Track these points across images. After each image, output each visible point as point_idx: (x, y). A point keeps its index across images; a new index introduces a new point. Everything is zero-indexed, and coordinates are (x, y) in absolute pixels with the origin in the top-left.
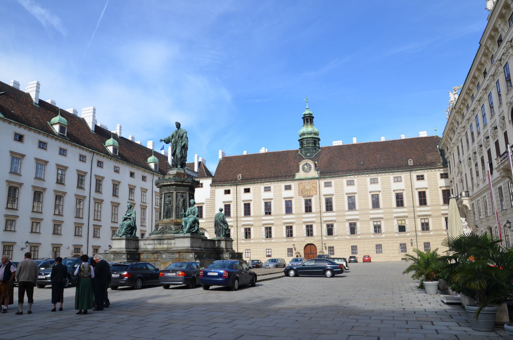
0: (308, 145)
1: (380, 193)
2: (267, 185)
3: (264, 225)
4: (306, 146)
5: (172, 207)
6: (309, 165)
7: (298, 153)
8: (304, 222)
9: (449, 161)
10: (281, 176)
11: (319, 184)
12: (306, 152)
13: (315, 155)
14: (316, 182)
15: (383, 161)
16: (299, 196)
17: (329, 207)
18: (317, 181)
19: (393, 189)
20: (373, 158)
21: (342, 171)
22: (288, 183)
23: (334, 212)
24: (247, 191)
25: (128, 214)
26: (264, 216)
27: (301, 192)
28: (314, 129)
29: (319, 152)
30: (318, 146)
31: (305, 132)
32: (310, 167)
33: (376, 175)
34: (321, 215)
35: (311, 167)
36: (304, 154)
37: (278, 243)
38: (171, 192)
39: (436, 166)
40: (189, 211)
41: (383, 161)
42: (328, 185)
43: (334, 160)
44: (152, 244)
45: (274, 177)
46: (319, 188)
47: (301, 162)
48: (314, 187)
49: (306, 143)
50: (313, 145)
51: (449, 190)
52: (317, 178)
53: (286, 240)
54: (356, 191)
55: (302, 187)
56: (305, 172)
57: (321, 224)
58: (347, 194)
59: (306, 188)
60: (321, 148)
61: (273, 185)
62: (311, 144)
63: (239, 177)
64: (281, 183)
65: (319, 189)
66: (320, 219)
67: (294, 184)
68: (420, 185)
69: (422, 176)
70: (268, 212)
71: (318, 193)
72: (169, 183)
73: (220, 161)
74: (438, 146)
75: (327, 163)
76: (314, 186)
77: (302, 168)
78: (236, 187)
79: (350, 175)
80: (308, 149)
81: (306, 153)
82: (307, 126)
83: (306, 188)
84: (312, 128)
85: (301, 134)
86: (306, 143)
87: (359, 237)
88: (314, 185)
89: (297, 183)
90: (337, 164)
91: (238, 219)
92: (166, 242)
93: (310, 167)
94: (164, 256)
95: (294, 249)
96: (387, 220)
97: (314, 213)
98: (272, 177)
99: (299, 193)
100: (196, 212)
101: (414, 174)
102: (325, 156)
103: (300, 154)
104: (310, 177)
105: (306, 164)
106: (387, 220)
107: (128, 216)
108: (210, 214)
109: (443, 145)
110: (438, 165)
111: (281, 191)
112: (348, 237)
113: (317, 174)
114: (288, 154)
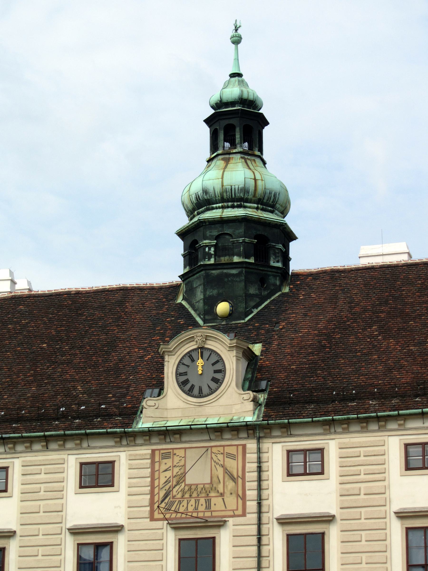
0: (224, 260)
4: (212, 261)
6: (214, 359)
7: (175, 297)
10: (64, 416)
11: (259, 458)
12: (215, 292)
13: (255, 311)
14: (244, 446)
16: (152, 519)
28: (258, 177)
29: (284, 294)
30: (280, 265)
31: (211, 190)
32: (218, 367)
35: (222, 371)
36: (201, 305)
43: (352, 339)
45: (31, 420)
46: (260, 480)
47: (173, 344)
49: (216, 246)
50: (252, 260)
55: (168, 474)
56: (190, 392)
59: (190, 479)
60: (296, 275)
62: (239, 255)
64: (63, 448)
65: (260, 488)
75: (312, 353)
76: (236, 477)
77: (178, 374)
80: (220, 278)
82: (227, 161)
83: (190, 479)
84: (249, 174)
85: (194, 200)
86: (216, 246)
88: (231, 464)
89: (146, 451)
90: (365, 354)
93: (216, 372)
102: (305, 315)
103: (184, 303)
104: (212, 421)
113: (250, 406)
114: (121, 303)
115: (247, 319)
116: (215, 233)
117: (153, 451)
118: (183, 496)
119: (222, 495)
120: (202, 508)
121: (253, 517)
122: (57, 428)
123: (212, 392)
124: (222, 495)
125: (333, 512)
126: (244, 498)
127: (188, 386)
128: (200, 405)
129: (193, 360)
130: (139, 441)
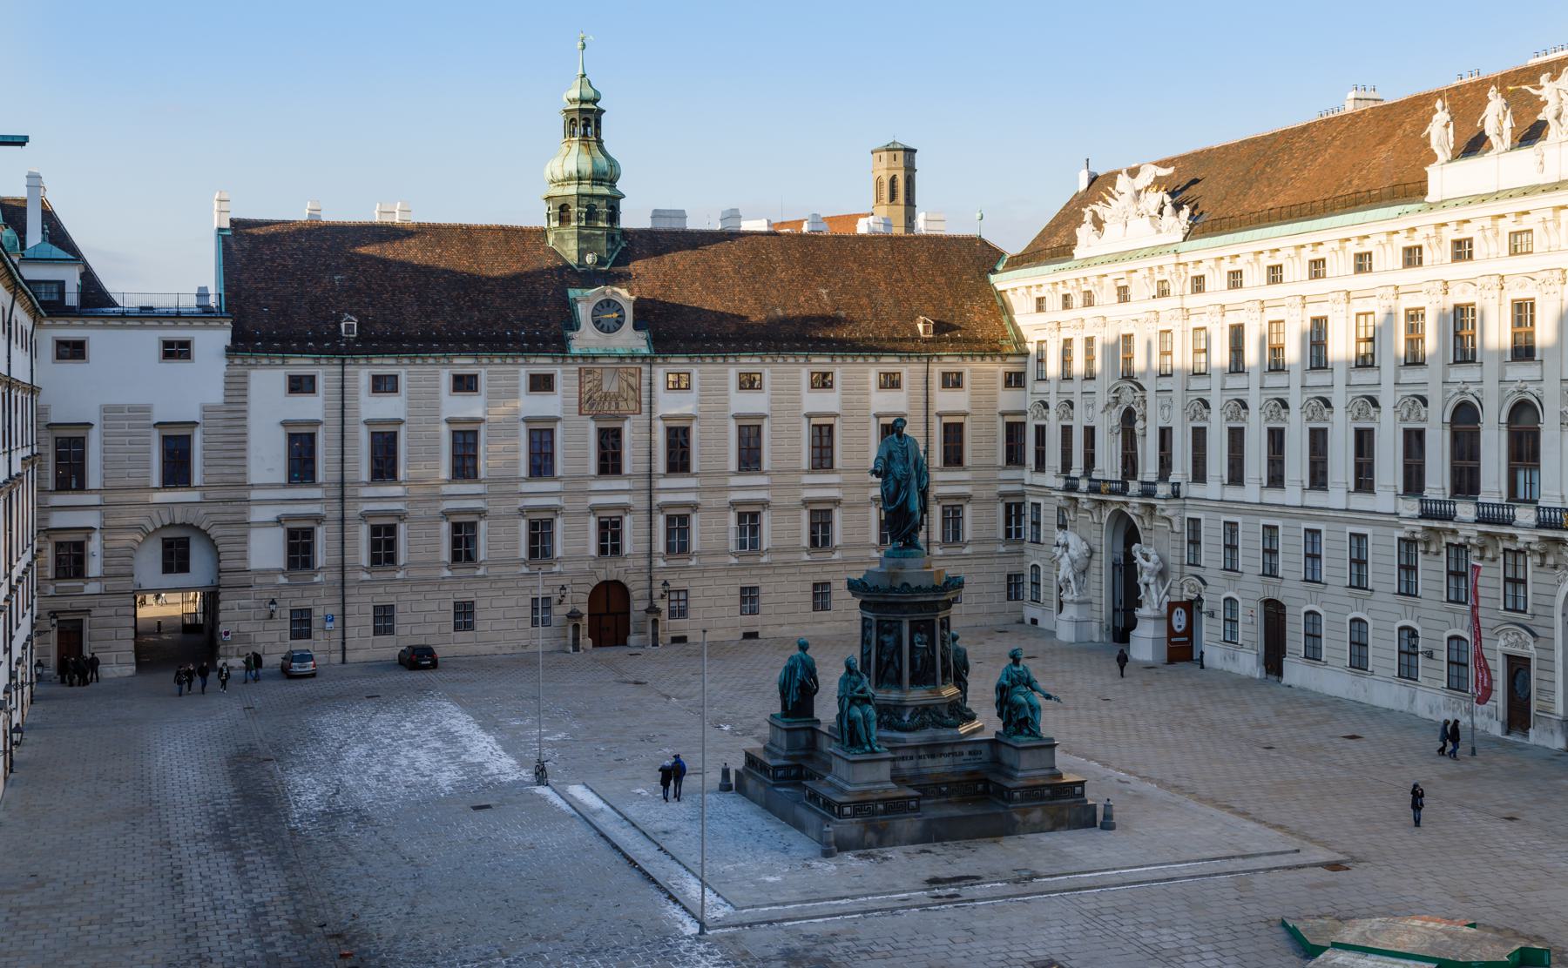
1: (838, 420)
2: (464, 364)
3: (446, 514)
5: (933, 658)
6: (617, 307)
8: (594, 509)
17: (679, 460)
18: (645, 368)
19: (874, 411)
20: (811, 299)
21: (725, 339)
22: (542, 365)
23: (693, 475)
24: (383, 385)
25: (860, 687)
27: (588, 404)
33: (828, 360)
34: (653, 484)
35: (622, 316)
37: (499, 579)
40: (1015, 676)
44: (911, 758)
48: (633, 390)
51: (1024, 424)
52: (644, 357)
53: (525, 570)
54: (765, 411)
55: (591, 385)
56: (601, 329)
57: (650, 511)
61: (487, 370)
63: (349, 327)
64: (515, 364)
65: (651, 396)
66: (646, 497)
67: (563, 372)
68: (948, 401)
69: (959, 374)
71: (645, 407)
73: (224, 237)
74: (993, 278)
78: (339, 369)
81: (581, 254)
83: (605, 390)
87: (764, 559)
88: (632, 380)
91: (348, 492)
92: (947, 750)
94: (1017, 794)
95: (555, 600)
96: (852, 506)
97: (629, 477)
98: (481, 340)
100: (1032, 679)
101: (937, 370)
104: (620, 351)
105: (608, 304)
106: (852, 506)
107: (859, 692)
108: (227, 471)
112: (734, 560)
113: (645, 342)
116: (585, 203)
117: (580, 369)
119: (626, 400)
120: (613, 408)
121: (645, 414)
123: (616, 330)
124: (626, 400)
126: (640, 403)
127: (600, 325)
129: (617, 311)
130: (570, 361)
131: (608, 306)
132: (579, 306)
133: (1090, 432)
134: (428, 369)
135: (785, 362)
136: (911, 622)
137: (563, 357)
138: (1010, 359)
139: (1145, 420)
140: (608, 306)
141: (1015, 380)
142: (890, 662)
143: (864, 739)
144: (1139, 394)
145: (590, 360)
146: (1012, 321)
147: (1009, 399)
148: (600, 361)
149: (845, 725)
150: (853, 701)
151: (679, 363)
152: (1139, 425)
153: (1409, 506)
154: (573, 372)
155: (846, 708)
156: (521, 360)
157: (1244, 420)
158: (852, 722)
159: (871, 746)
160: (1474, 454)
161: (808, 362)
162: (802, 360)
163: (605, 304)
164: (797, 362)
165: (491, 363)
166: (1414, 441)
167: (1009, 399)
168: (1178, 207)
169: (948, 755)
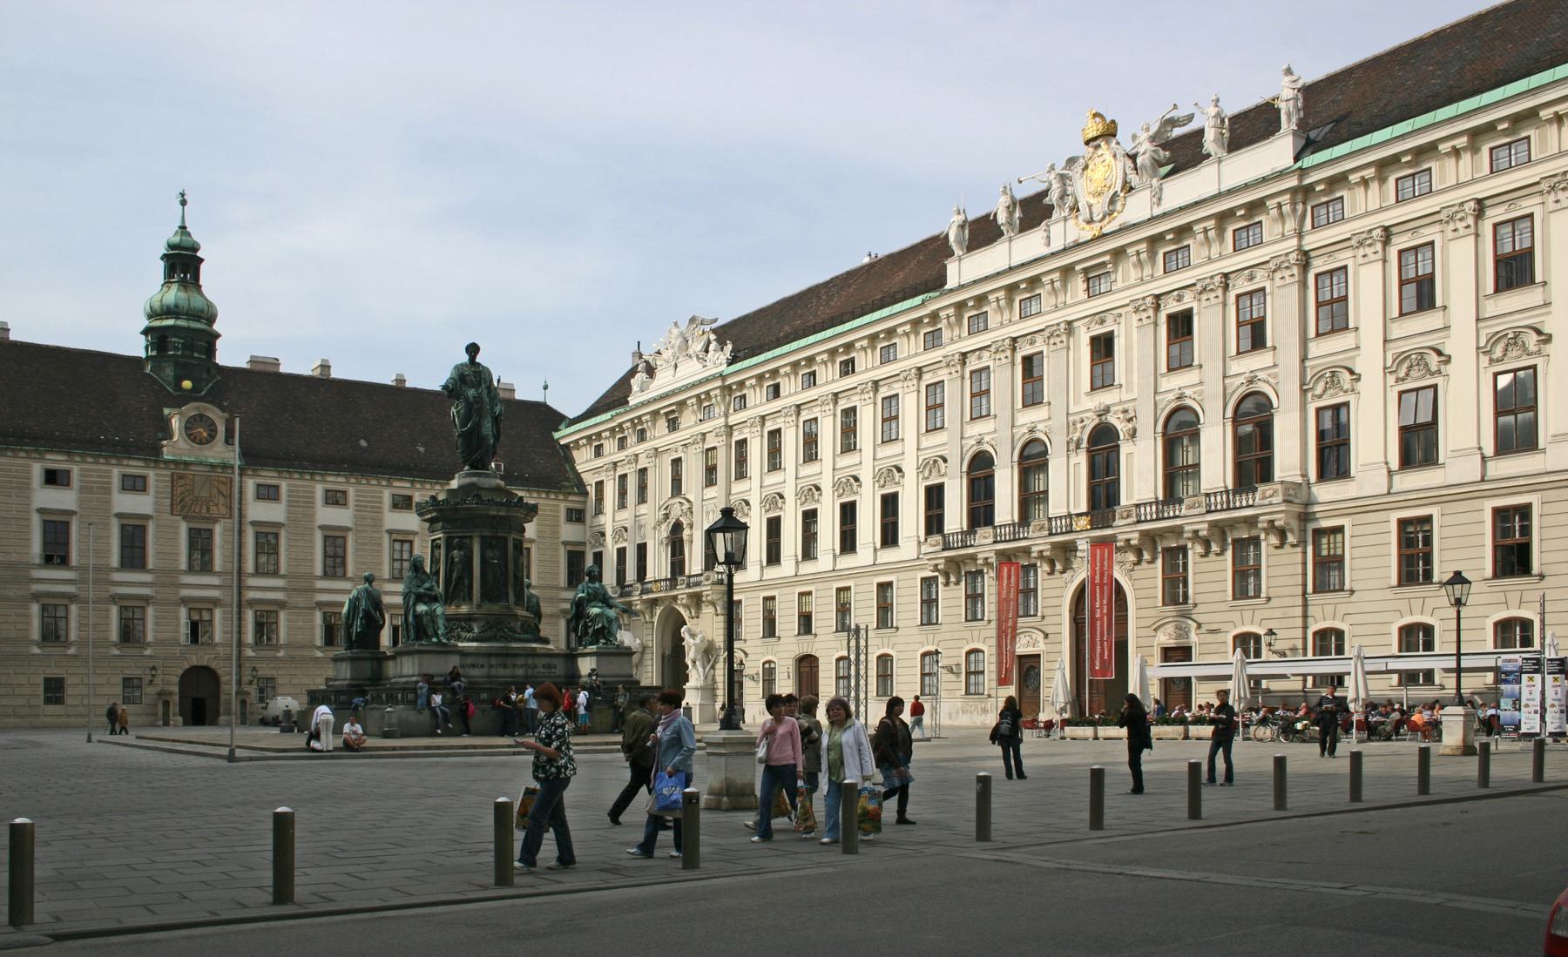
2: (57, 461)
5: (505, 575)
6: (209, 423)
9: (600, 485)
13: (206, 389)
15: (422, 449)
16: (172, 514)
22: (135, 467)
25: (427, 585)
26: (40, 566)
32: (213, 428)
33: (408, 485)
35: (215, 431)
38: (499, 534)
39: (560, 489)
41: (422, 449)
42: (268, 494)
51: (582, 554)
54: (350, 524)
55: (183, 488)
56: (194, 441)
58: (322, 528)
67: (156, 475)
70: (56, 554)
72: (502, 513)
79: (337, 475)
88: (222, 488)
89: (168, 472)
99: (172, 505)
105: (201, 416)
107: (426, 589)
109: (589, 438)
110: (567, 487)
111: (108, 491)
115: (204, 393)
117: (172, 474)
118: (192, 503)
120: (204, 511)
122: (106, 451)
125: (282, 521)
126: (231, 508)
128: (200, 449)
130: (162, 466)
131: (201, 420)
132: (173, 421)
133: (642, 549)
134: (19, 461)
135: (369, 484)
136: (483, 538)
137: (156, 461)
138: (571, 498)
139: (691, 528)
140: (201, 420)
141: (576, 516)
142: (460, 578)
143: (430, 631)
144: (687, 505)
145: (182, 467)
146: (574, 469)
147: (569, 532)
148: (193, 468)
149: (411, 619)
150: (420, 598)
151: (268, 477)
152: (686, 532)
153: (933, 543)
154: (166, 476)
155: (411, 603)
156: (114, 461)
157: (781, 509)
158: (417, 617)
159: (438, 637)
160: (990, 494)
161: (390, 486)
162: (384, 483)
163: (198, 419)
164: (379, 485)
165: (84, 462)
166: (935, 496)
167: (569, 532)
168: (722, 343)
169: (522, 666)
